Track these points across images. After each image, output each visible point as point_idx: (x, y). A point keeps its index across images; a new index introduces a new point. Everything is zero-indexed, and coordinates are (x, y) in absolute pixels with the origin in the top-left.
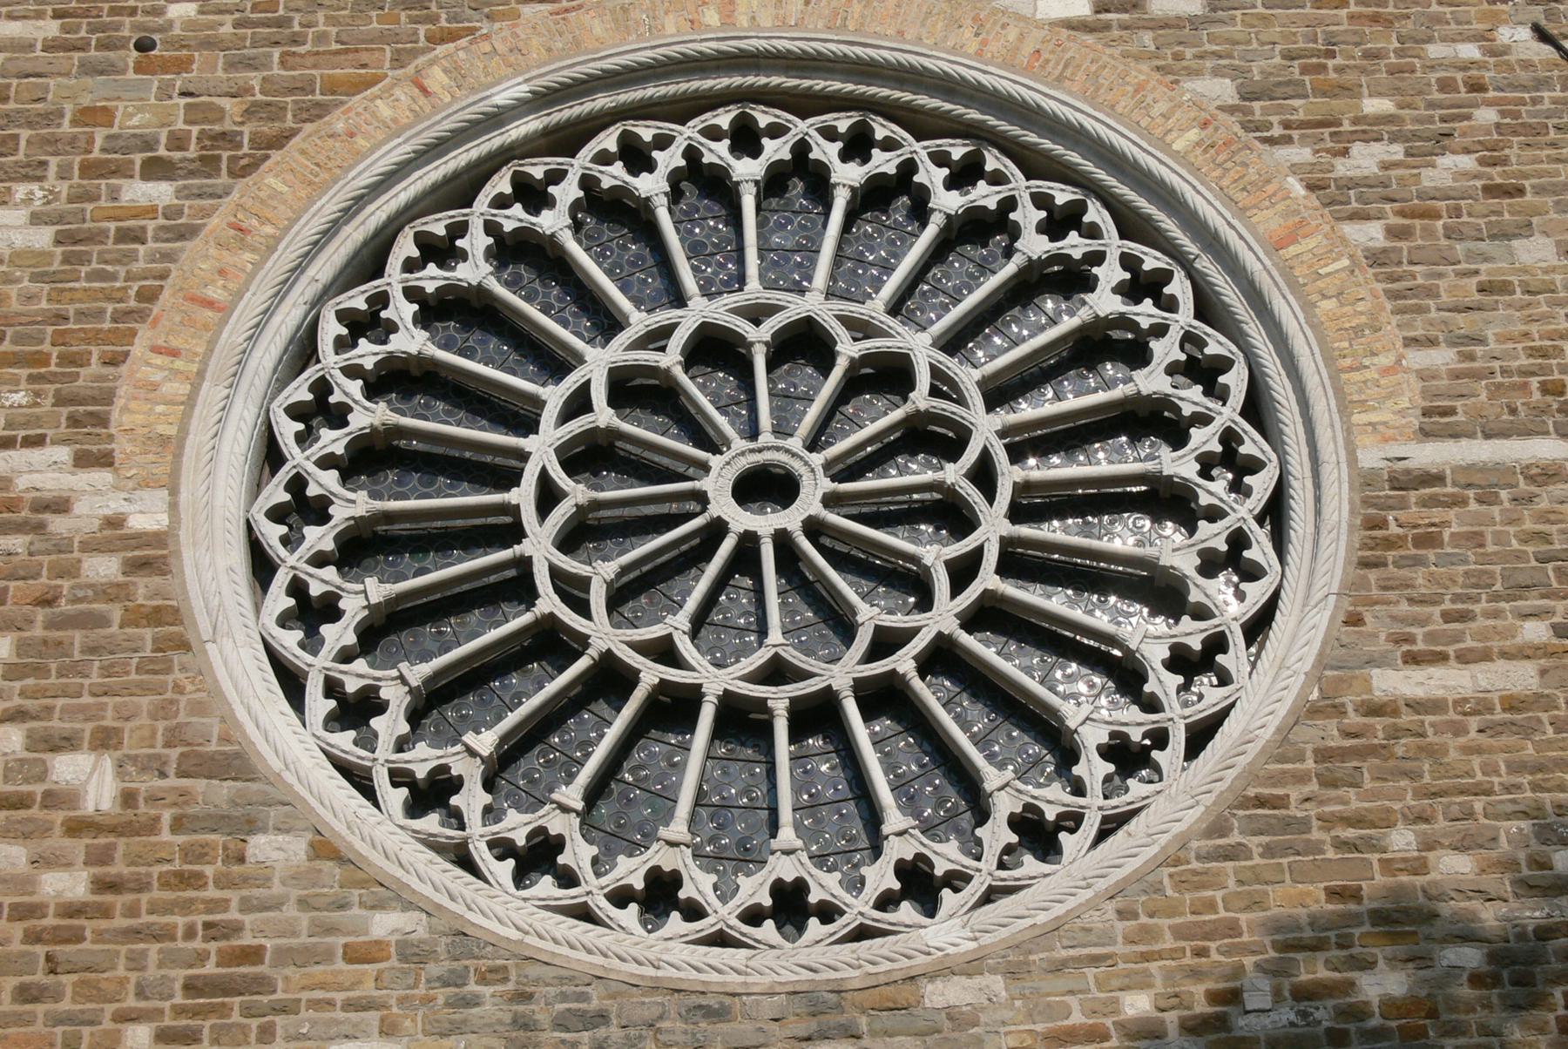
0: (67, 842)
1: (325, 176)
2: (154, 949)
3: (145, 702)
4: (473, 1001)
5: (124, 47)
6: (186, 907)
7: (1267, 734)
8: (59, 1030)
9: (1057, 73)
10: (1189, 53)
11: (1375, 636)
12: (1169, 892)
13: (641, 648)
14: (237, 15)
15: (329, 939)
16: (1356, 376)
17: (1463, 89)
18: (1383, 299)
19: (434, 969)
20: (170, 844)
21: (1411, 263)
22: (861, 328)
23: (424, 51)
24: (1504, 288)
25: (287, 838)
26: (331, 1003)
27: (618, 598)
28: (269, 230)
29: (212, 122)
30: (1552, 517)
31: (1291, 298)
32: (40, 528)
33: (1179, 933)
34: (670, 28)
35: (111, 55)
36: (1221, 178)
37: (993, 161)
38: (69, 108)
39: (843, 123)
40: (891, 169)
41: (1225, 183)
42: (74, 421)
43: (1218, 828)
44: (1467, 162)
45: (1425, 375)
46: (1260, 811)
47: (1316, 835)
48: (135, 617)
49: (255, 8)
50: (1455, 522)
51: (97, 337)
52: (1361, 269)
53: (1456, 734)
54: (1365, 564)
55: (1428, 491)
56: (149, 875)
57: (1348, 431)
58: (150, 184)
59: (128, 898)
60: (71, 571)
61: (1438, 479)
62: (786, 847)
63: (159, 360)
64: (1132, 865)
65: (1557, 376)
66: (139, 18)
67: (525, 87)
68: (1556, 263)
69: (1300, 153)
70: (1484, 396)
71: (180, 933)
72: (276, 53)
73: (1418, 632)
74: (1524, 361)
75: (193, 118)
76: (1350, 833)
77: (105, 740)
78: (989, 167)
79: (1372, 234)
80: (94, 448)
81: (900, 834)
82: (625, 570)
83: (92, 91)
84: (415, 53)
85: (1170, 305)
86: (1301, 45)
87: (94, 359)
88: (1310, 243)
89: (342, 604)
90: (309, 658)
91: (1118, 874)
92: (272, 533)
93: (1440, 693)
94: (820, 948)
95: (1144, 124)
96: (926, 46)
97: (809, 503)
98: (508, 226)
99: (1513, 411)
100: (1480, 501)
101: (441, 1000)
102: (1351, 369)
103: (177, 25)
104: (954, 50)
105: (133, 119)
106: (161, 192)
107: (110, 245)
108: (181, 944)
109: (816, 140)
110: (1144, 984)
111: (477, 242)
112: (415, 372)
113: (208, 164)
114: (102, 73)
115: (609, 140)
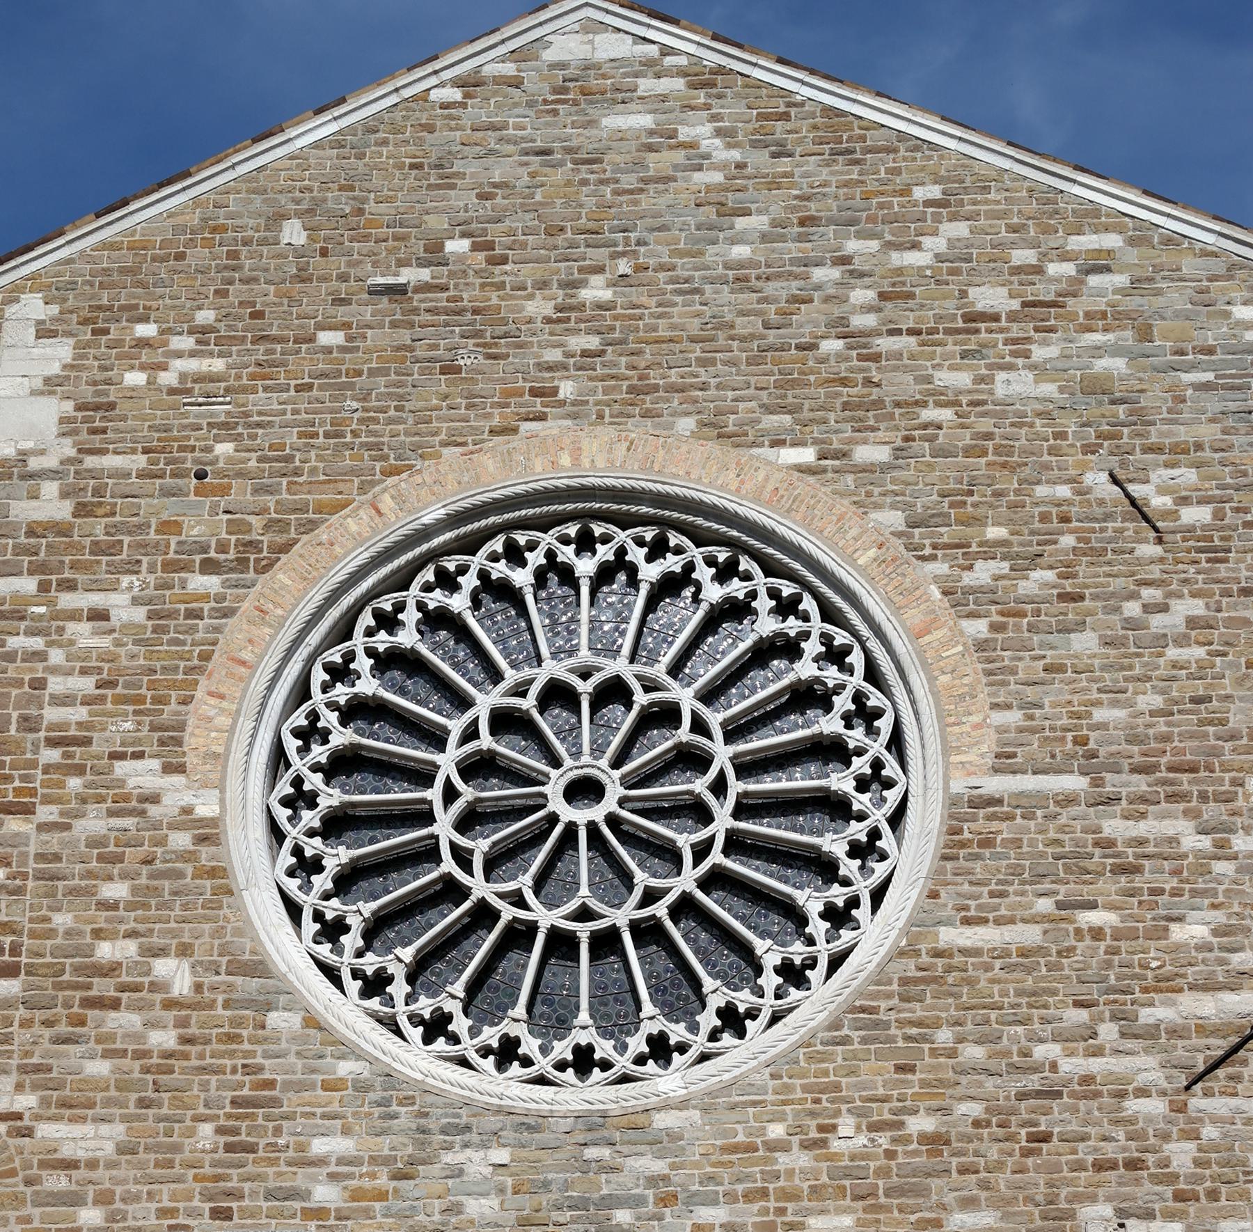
0: (164, 1013)
1: (315, 573)
2: (214, 1079)
3: (207, 927)
4: (394, 1116)
5: (188, 476)
6: (232, 1054)
7: (871, 967)
8: (161, 1125)
9: (788, 506)
10: (877, 491)
11: (945, 905)
12: (802, 1064)
13: (501, 896)
14: (260, 453)
15: (314, 1076)
16: (956, 729)
17: (1055, 521)
18: (981, 675)
19: (372, 1096)
20: (223, 1016)
21: (1002, 649)
22: (650, 686)
23: (381, 481)
24: (1061, 669)
25: (290, 1014)
26: (314, 1114)
27: (491, 865)
28: (279, 612)
29: (244, 533)
30: (1067, 829)
31: (921, 673)
32: (142, 813)
33: (806, 1089)
34: (539, 469)
35: (179, 481)
36: (886, 585)
37: (745, 564)
38: (153, 522)
39: (649, 534)
40: (677, 569)
41: (889, 588)
42: (162, 743)
43: (835, 1025)
44: (1050, 575)
45: (1001, 730)
46: (862, 1015)
47: (893, 1031)
48: (201, 873)
49: (271, 446)
50: (1005, 831)
51: (174, 685)
52: (971, 655)
53: (986, 971)
54: (945, 858)
55: (991, 809)
56: (211, 1034)
57: (947, 766)
58: (206, 578)
59: (199, 1048)
60: (161, 842)
61: (999, 802)
62: (583, 1024)
63: (212, 701)
64: (783, 1045)
65: (1085, 732)
66: (197, 454)
67: (443, 511)
68: (1096, 651)
70: (1035, 746)
71: (228, 1071)
72: (284, 481)
73: (972, 903)
74: (1065, 721)
75: (232, 530)
76: (914, 1031)
77: (184, 951)
78: (741, 568)
79: (979, 628)
80: (174, 761)
81: (651, 1018)
82: (495, 844)
83: (169, 509)
84: (373, 484)
85: (850, 670)
86: (952, 486)
87: (173, 700)
88: (938, 634)
89: (324, 862)
90: (304, 897)
91: (773, 1052)
92: (282, 814)
93: (980, 944)
94: (597, 1088)
95: (840, 545)
96: (703, 484)
97: (609, 804)
98: (432, 605)
99: (1053, 756)
100: (1023, 817)
101: (376, 1115)
102: (954, 724)
103: (221, 460)
104: (722, 488)
105: (195, 531)
106: (211, 583)
107: (181, 621)
108: (229, 1077)
109: (631, 546)
110: (778, 1118)
111: (411, 616)
112: (371, 704)
113: (242, 563)
114: (173, 495)
115: (497, 545)
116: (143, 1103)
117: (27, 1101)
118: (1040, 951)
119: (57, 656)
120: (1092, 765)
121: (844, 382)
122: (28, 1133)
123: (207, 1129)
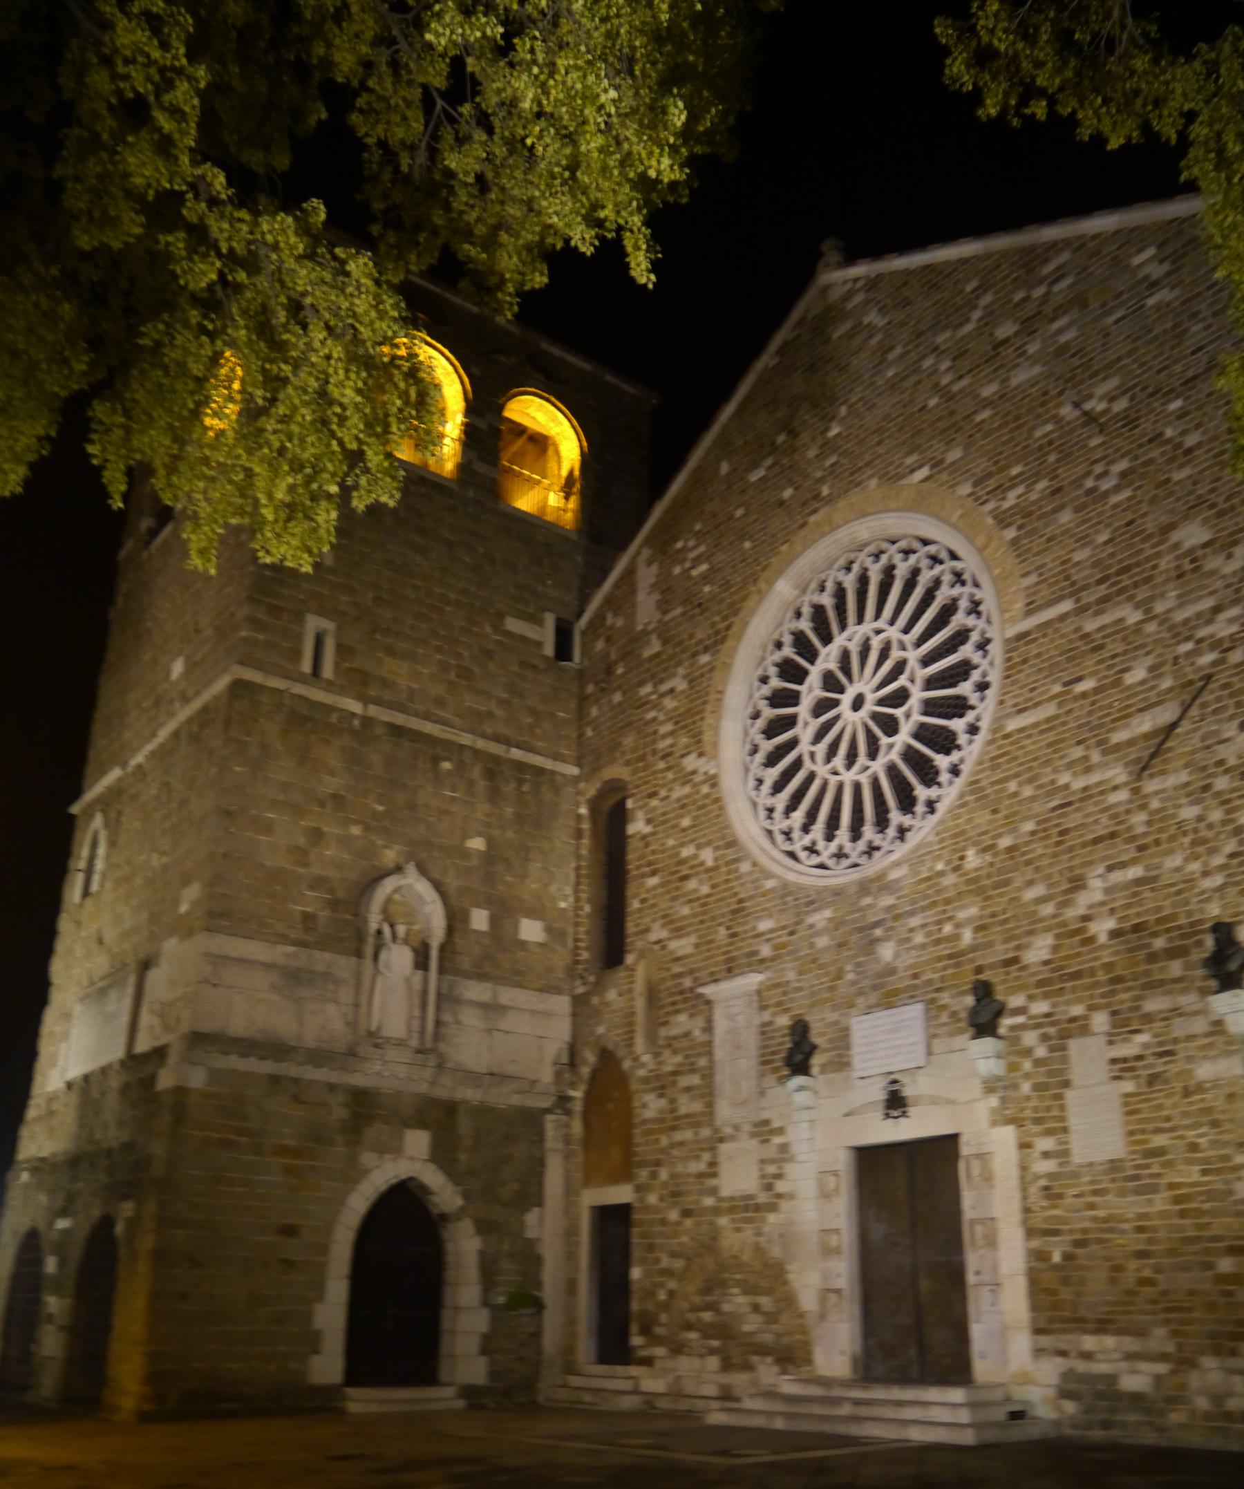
43: (962, 795)
54: (1007, 677)
57: (1003, 622)
105: (700, 635)
110: (939, 858)
119: (661, 717)
120: (1075, 591)
122: (664, 948)
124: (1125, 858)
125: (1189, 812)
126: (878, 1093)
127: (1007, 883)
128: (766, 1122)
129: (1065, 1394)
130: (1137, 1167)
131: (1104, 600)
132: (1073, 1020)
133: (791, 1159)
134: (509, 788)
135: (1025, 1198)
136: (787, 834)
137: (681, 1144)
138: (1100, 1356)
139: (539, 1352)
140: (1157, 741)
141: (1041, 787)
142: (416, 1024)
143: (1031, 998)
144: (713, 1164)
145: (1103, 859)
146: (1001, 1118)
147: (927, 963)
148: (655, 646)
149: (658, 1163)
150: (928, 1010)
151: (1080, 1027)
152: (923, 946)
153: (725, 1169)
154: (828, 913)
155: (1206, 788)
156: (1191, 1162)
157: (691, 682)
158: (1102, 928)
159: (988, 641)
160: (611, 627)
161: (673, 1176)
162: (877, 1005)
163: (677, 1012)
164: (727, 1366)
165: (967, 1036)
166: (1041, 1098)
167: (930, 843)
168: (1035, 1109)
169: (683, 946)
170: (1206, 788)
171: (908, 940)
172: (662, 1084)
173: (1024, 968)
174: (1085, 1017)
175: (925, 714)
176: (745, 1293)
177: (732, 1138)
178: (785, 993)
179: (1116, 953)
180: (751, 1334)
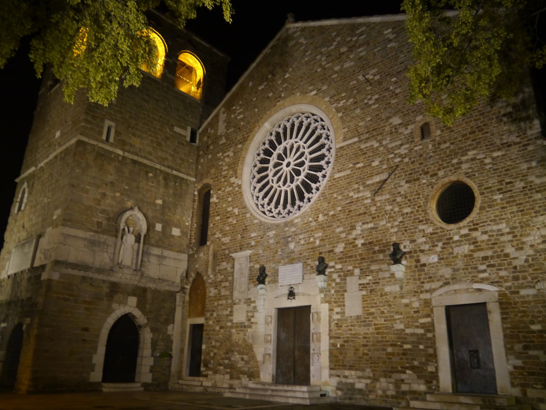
43: (319, 197)
45: (344, 133)
57: (336, 142)
61: (343, 147)
69: (335, 105)
79: (340, 115)
105: (239, 138)
110: (311, 216)
116: (233, 232)
117: (220, 235)
118: (350, 174)
119: (224, 164)
121: (320, 76)
122: (220, 240)
123: (239, 235)
124: (368, 221)
125: (388, 208)
126: (286, 291)
127: (331, 226)
128: (250, 299)
129: (338, 389)
130: (365, 318)
131: (368, 139)
132: (349, 271)
133: (257, 311)
134: (172, 184)
135: (330, 326)
136: (263, 206)
137: (222, 305)
138: (350, 377)
139: (170, 372)
140: (380, 184)
141: (344, 196)
142: (134, 261)
143: (336, 263)
144: (231, 312)
145: (361, 221)
146: (324, 301)
147: (304, 250)
148: (224, 141)
149: (213, 311)
150: (304, 265)
151: (351, 273)
152: (304, 245)
153: (235, 313)
154: (274, 232)
155: (394, 201)
156: (381, 317)
157: (234, 153)
158: (360, 242)
159: (331, 148)
160: (210, 133)
161: (217, 315)
162: (288, 263)
163: (224, 261)
164: (232, 378)
165: (315, 274)
166: (337, 295)
167: (308, 212)
168: (335, 298)
169: (226, 240)
170: (394, 201)
171: (299, 242)
172: (216, 285)
173: (335, 253)
174: (353, 270)
175: (309, 170)
176: (239, 354)
177: (238, 304)
178: (258, 257)
179: (363, 251)
180: (240, 368)
